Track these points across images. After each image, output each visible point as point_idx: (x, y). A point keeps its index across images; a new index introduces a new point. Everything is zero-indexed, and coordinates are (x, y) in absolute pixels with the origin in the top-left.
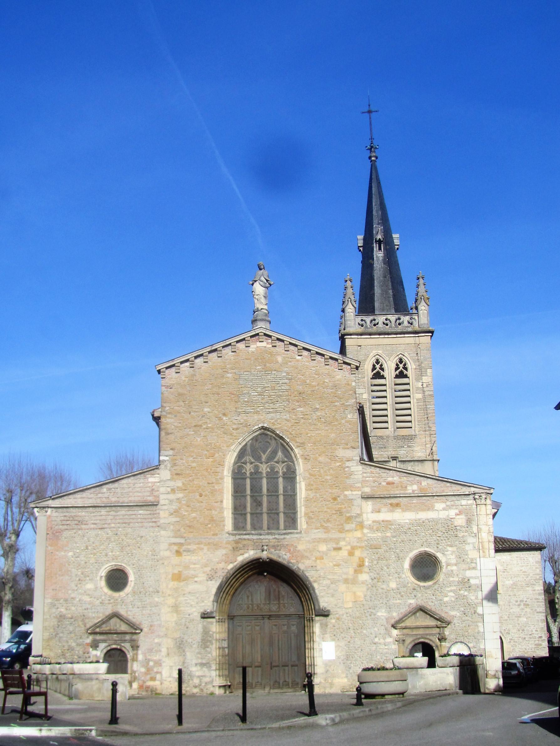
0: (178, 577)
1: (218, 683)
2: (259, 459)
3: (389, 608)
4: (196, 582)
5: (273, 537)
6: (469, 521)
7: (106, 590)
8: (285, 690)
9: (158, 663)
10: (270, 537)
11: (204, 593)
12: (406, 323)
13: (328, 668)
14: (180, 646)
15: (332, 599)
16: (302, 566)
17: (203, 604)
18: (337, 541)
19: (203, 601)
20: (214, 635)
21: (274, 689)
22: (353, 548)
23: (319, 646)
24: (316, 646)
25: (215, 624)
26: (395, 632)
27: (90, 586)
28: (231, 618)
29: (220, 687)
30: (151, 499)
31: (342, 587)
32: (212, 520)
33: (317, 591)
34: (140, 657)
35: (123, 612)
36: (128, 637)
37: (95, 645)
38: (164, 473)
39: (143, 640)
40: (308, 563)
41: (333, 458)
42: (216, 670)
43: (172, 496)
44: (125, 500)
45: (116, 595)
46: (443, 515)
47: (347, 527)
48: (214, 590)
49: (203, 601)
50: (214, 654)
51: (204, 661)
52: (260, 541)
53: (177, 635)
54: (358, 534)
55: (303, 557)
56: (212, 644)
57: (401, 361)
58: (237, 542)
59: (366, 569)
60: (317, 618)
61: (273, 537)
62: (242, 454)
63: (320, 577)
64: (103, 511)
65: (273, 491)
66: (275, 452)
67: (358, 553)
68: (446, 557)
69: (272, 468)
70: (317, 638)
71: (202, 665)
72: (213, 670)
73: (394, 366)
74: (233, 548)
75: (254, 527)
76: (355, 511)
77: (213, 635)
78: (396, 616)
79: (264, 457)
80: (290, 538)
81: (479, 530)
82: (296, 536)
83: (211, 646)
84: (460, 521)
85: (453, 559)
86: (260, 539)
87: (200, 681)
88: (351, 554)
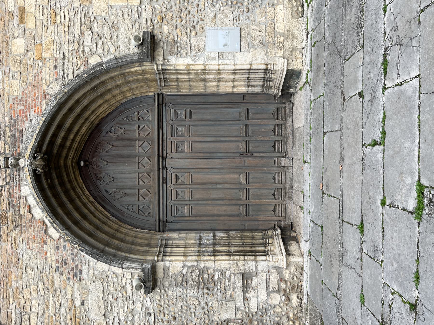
1: (280, 257)
4: (83, 303)
13: (255, 43)
16: (54, 89)
17: (129, 287)
19: (123, 287)
20: (189, 264)
21: (286, 151)
23: (214, 59)
24: (213, 66)
29: (288, 253)
33: (105, 59)
40: (47, 75)
42: (255, 261)
48: (102, 266)
49: (123, 287)
51: (239, 284)
60: (160, 60)
74: (16, 227)
77: (189, 267)
87: (278, 292)
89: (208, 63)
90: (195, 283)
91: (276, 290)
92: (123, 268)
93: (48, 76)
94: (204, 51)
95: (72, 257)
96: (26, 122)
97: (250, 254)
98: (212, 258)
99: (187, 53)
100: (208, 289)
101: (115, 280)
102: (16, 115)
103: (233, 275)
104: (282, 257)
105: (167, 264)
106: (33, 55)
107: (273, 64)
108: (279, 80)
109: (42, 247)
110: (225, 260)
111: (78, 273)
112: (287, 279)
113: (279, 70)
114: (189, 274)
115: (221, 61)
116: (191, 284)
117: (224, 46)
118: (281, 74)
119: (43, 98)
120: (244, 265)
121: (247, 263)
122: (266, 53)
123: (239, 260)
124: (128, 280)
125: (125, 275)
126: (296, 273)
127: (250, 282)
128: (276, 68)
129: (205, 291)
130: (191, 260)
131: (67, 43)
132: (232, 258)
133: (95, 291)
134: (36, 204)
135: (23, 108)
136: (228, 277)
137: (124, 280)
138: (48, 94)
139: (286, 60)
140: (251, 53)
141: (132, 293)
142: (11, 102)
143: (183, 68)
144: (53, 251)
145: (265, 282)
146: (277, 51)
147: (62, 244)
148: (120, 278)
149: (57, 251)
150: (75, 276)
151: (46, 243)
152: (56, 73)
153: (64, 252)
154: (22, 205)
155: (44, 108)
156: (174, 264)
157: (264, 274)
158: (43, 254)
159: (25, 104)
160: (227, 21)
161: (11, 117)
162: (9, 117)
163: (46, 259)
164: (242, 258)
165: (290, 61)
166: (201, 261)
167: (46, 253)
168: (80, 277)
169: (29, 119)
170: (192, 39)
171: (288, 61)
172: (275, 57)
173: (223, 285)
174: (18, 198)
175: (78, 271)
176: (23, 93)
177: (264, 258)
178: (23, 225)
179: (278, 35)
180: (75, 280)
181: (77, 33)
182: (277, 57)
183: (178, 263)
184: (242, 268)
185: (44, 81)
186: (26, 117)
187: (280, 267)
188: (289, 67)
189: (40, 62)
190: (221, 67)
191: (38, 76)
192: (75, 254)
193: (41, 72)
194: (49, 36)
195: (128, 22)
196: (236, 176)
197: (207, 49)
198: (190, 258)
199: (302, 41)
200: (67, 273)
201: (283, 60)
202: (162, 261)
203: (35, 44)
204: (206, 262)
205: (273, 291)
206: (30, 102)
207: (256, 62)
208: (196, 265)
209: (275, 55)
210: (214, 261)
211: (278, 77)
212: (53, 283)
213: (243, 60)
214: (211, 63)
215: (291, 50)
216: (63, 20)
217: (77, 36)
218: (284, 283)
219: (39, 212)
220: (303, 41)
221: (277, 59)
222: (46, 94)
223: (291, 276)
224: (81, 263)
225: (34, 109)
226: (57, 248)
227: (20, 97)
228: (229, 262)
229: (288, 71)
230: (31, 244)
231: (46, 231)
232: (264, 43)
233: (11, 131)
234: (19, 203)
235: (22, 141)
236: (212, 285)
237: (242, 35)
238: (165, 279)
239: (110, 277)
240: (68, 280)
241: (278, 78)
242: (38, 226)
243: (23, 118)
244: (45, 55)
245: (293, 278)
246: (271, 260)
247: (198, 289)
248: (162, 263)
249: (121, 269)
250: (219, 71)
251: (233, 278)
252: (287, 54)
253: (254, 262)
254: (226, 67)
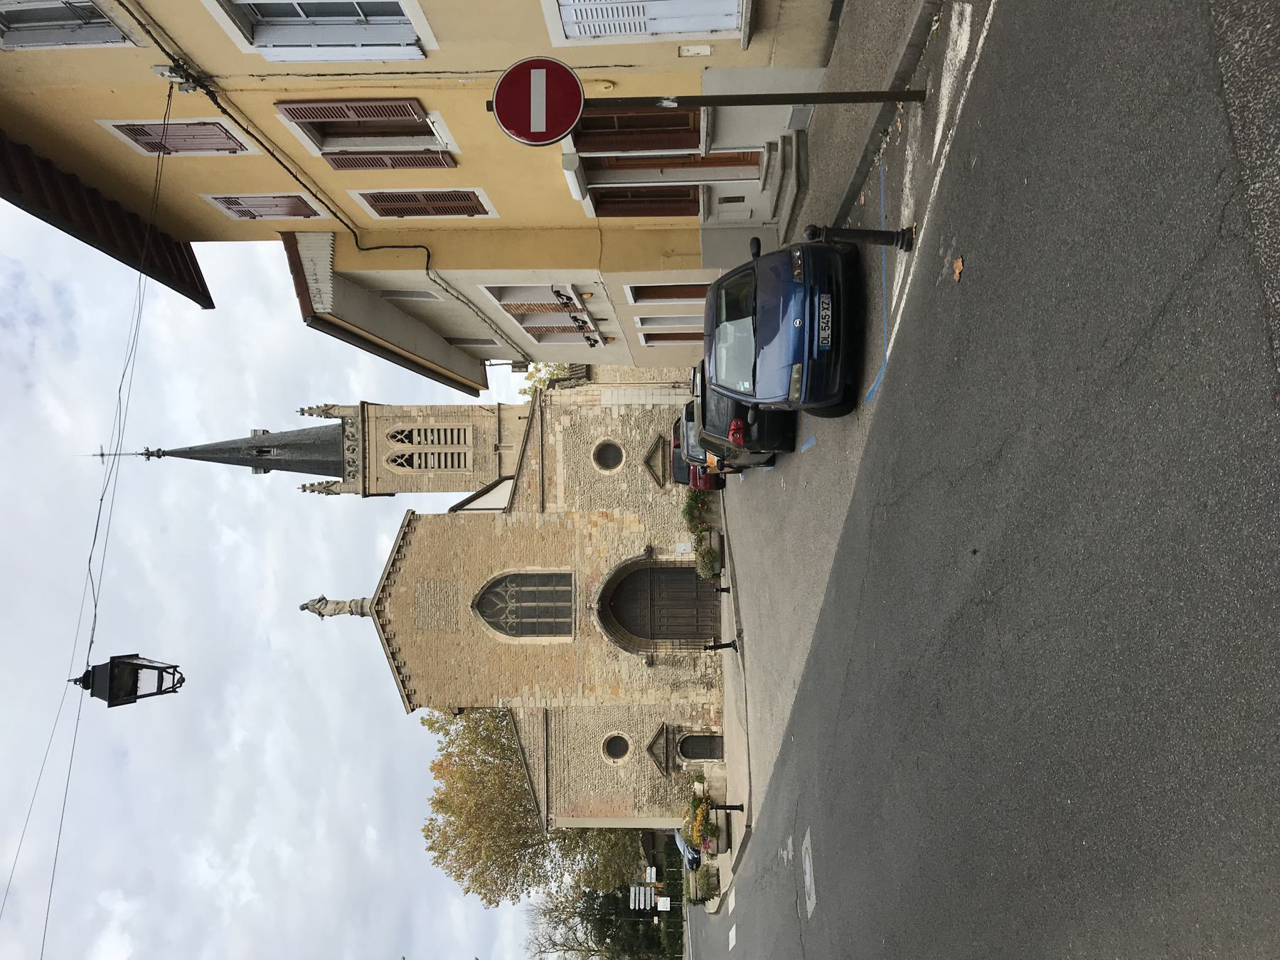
0: (615, 688)
2: (502, 610)
3: (645, 490)
6: (567, 412)
7: (626, 758)
9: (694, 707)
11: (630, 663)
12: (353, 430)
14: (676, 686)
16: (606, 571)
18: (583, 537)
22: (590, 522)
26: (668, 486)
27: (622, 773)
28: (653, 637)
30: (541, 716)
31: (625, 533)
32: (562, 656)
34: (688, 724)
35: (647, 742)
36: (671, 736)
37: (680, 767)
38: (516, 703)
39: (674, 720)
40: (603, 565)
41: (503, 538)
43: (538, 695)
44: (541, 742)
45: (631, 748)
46: (560, 437)
47: (569, 526)
48: (628, 654)
53: (668, 688)
54: (577, 517)
55: (597, 569)
57: (394, 437)
58: (583, 633)
59: (609, 511)
62: (497, 626)
64: (551, 762)
65: (533, 596)
66: (497, 594)
67: (594, 518)
68: (599, 436)
69: (512, 597)
70: (672, 558)
71: (695, 666)
73: (400, 445)
75: (569, 615)
76: (554, 518)
78: (652, 485)
79: (501, 605)
80: (579, 581)
81: (575, 403)
84: (566, 420)
85: (601, 429)
88: (596, 525)
106: (596, 554)
133: (625, 666)
156: (662, 653)
194: (604, 546)
203: (597, 551)
219: (598, 629)
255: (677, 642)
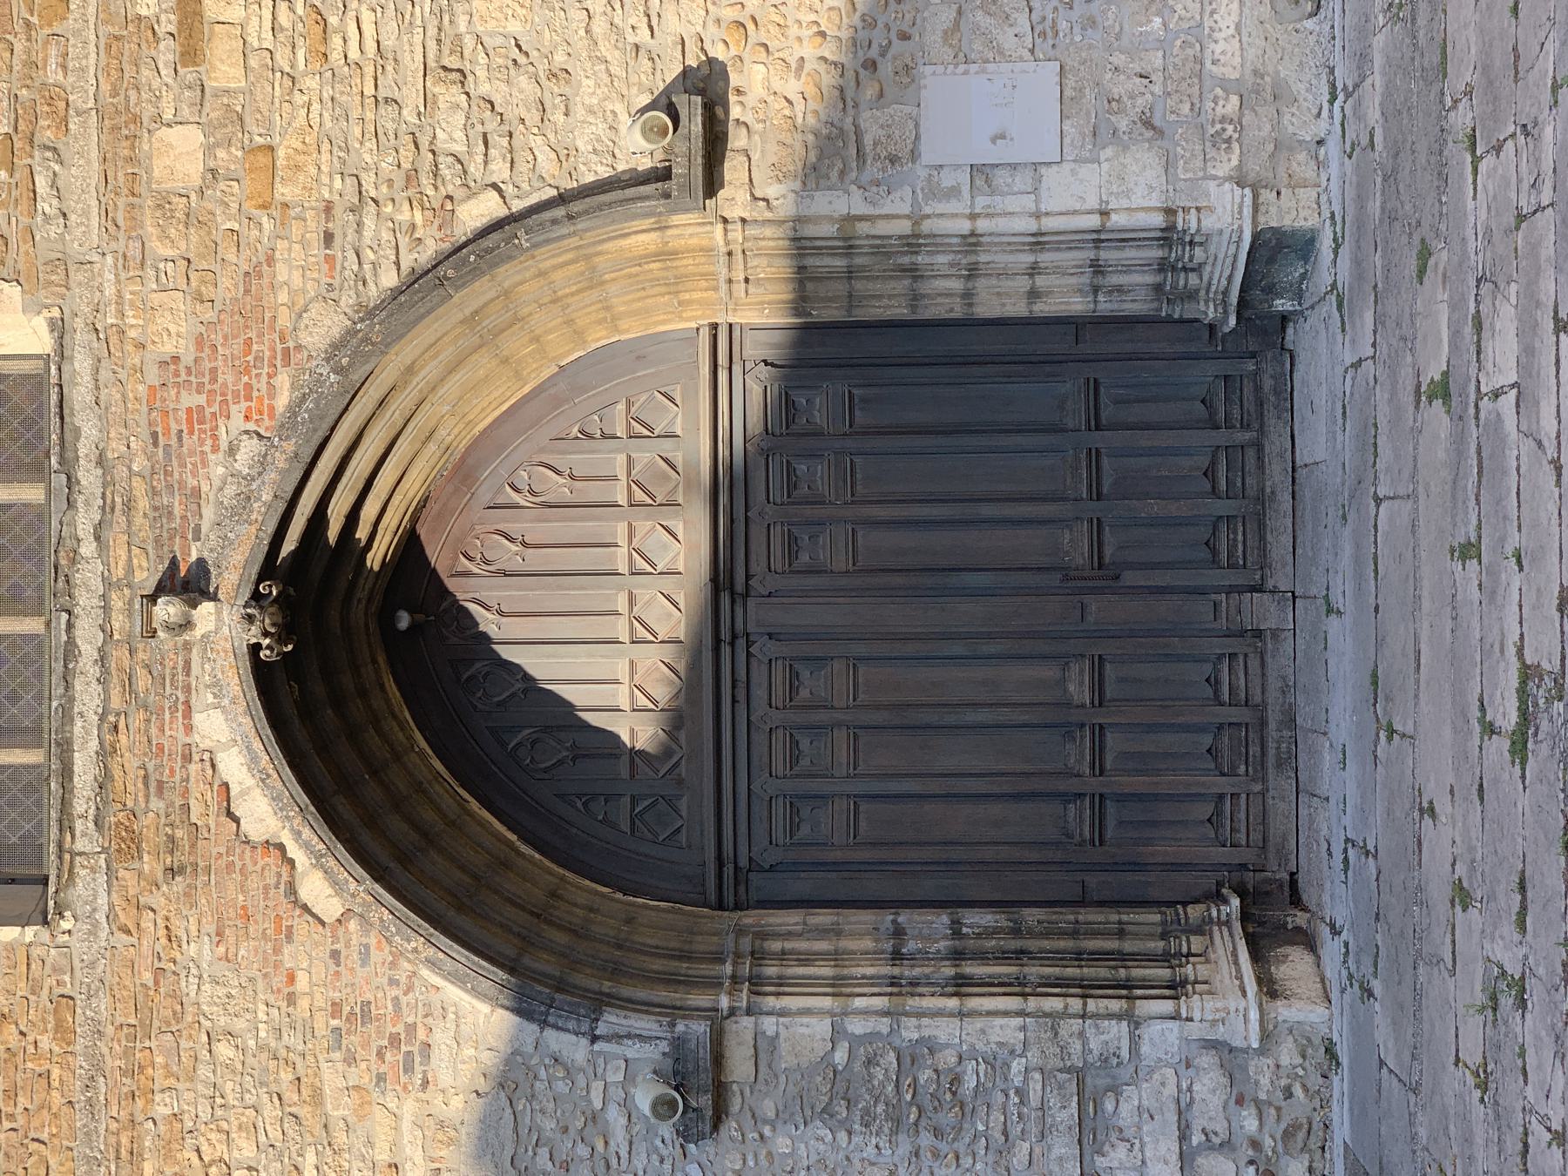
1: (1234, 1002)
5: (88, 549)
8: (1277, 474)
10: (89, 576)
13: (1123, 124)
15: (588, 89)
19: (594, 1118)
20: (857, 1026)
23: (954, 192)
24: (949, 219)
25: (769, 1024)
29: (1270, 989)
40: (296, 269)
42: (1127, 1016)
49: (594, 1118)
50: (1006, 1031)
52: (119, 655)
55: (251, 304)
56: (931, 1046)
58: (127, 845)
61: (88, 549)
63: (412, 177)
72: (1135, 1041)
82: (81, 363)
83: (948, 1058)
86: (102, 659)
87: (1227, 1146)
89: (927, 210)
90: (880, 1108)
91: (1216, 1140)
92: (594, 1039)
93: (297, 274)
94: (914, 162)
95: (394, 992)
96: (212, 457)
97: (1110, 992)
98: (953, 1003)
99: (842, 173)
100: (937, 1133)
101: (562, 1087)
102: (174, 427)
103: (1037, 1076)
104: (1242, 1004)
105: (769, 1024)
107: (1198, 209)
108: (1224, 269)
109: (277, 951)
110: (1006, 1014)
111: (417, 1059)
112: (1263, 1096)
113: (1221, 232)
114: (858, 1066)
115: (981, 202)
116: (866, 1111)
117: (994, 140)
118: (1233, 248)
119: (279, 363)
120: (1081, 1034)
121: (1097, 1026)
122: (1168, 167)
123: (1065, 1014)
124: (611, 1089)
125: (600, 1071)
126: (1301, 1072)
127: (1109, 1106)
128: (1209, 223)
129: (926, 1139)
130: (866, 1013)
131: (372, 145)
132: (1033, 1004)
134: (251, 782)
135: (201, 400)
136: (1018, 1081)
137: (597, 1086)
138: (299, 348)
139: (1247, 191)
140: (1105, 166)
141: (631, 1143)
142: (153, 376)
143: (829, 230)
144: (319, 972)
145: (1173, 1106)
146: (1211, 153)
147: (354, 942)
148: (581, 1081)
149: (333, 968)
150: (406, 1071)
151: (289, 938)
152: (330, 260)
153: (361, 972)
154: (196, 788)
155: (282, 401)
156: (801, 1027)
157: (1170, 1072)
158: (279, 981)
159: (208, 387)
160: (1007, 40)
161: (155, 435)
162: (145, 433)
163: (291, 999)
164: (1075, 1004)
165: (1267, 196)
166: (907, 1014)
167: (291, 979)
168: (425, 1072)
169: (224, 445)
170: (866, 114)
171: (1256, 196)
172: (1205, 178)
173: (997, 1118)
174: (183, 756)
175: (415, 1049)
176: (200, 342)
177: (1167, 1006)
178: (201, 864)
179: (1219, 91)
180: (405, 1088)
181: (412, 99)
182: (1215, 178)
183: (813, 1020)
184: (1077, 1046)
185: (283, 297)
186: (215, 437)
187: (1238, 1042)
188: (1261, 219)
189: (265, 219)
190: (983, 225)
191: (260, 276)
192: (403, 980)
193: (270, 261)
195: (614, 56)
196: (1049, 672)
197: (928, 156)
198: (859, 1003)
199: (1315, 111)
200: (374, 1057)
201: (1238, 191)
202: (749, 1012)
204: (925, 1021)
205: (1209, 1146)
206: (230, 379)
207: (1125, 203)
208: (885, 1030)
209: (1204, 169)
210: (961, 1015)
211: (1221, 256)
212: (317, 1097)
213: (1076, 193)
214: (941, 207)
215: (1270, 147)
216: (354, 54)
217: (409, 115)
218: (1254, 1111)
220: (1319, 114)
221: (1212, 185)
222: (291, 344)
223: (1284, 1082)
224: (426, 1016)
225: (244, 405)
226: (335, 955)
227: (187, 359)
228: (1019, 1021)
229: (1256, 236)
230: (232, 940)
231: (292, 890)
232: (1157, 122)
233: (155, 492)
234: (187, 780)
235: (197, 530)
236: (948, 1118)
237: (1068, 93)
238: (760, 1086)
239: (543, 1074)
240: (377, 1085)
241: (1220, 262)
242: (258, 868)
243: (202, 442)
244: (284, 192)
245: (1288, 1093)
246: (1197, 1015)
247: (895, 1132)
248: (747, 1022)
249: (584, 1042)
250: (972, 242)
251: (1039, 1087)
252: (1254, 169)
253: (1125, 1023)
254: (1001, 224)
255: (929, 929)
